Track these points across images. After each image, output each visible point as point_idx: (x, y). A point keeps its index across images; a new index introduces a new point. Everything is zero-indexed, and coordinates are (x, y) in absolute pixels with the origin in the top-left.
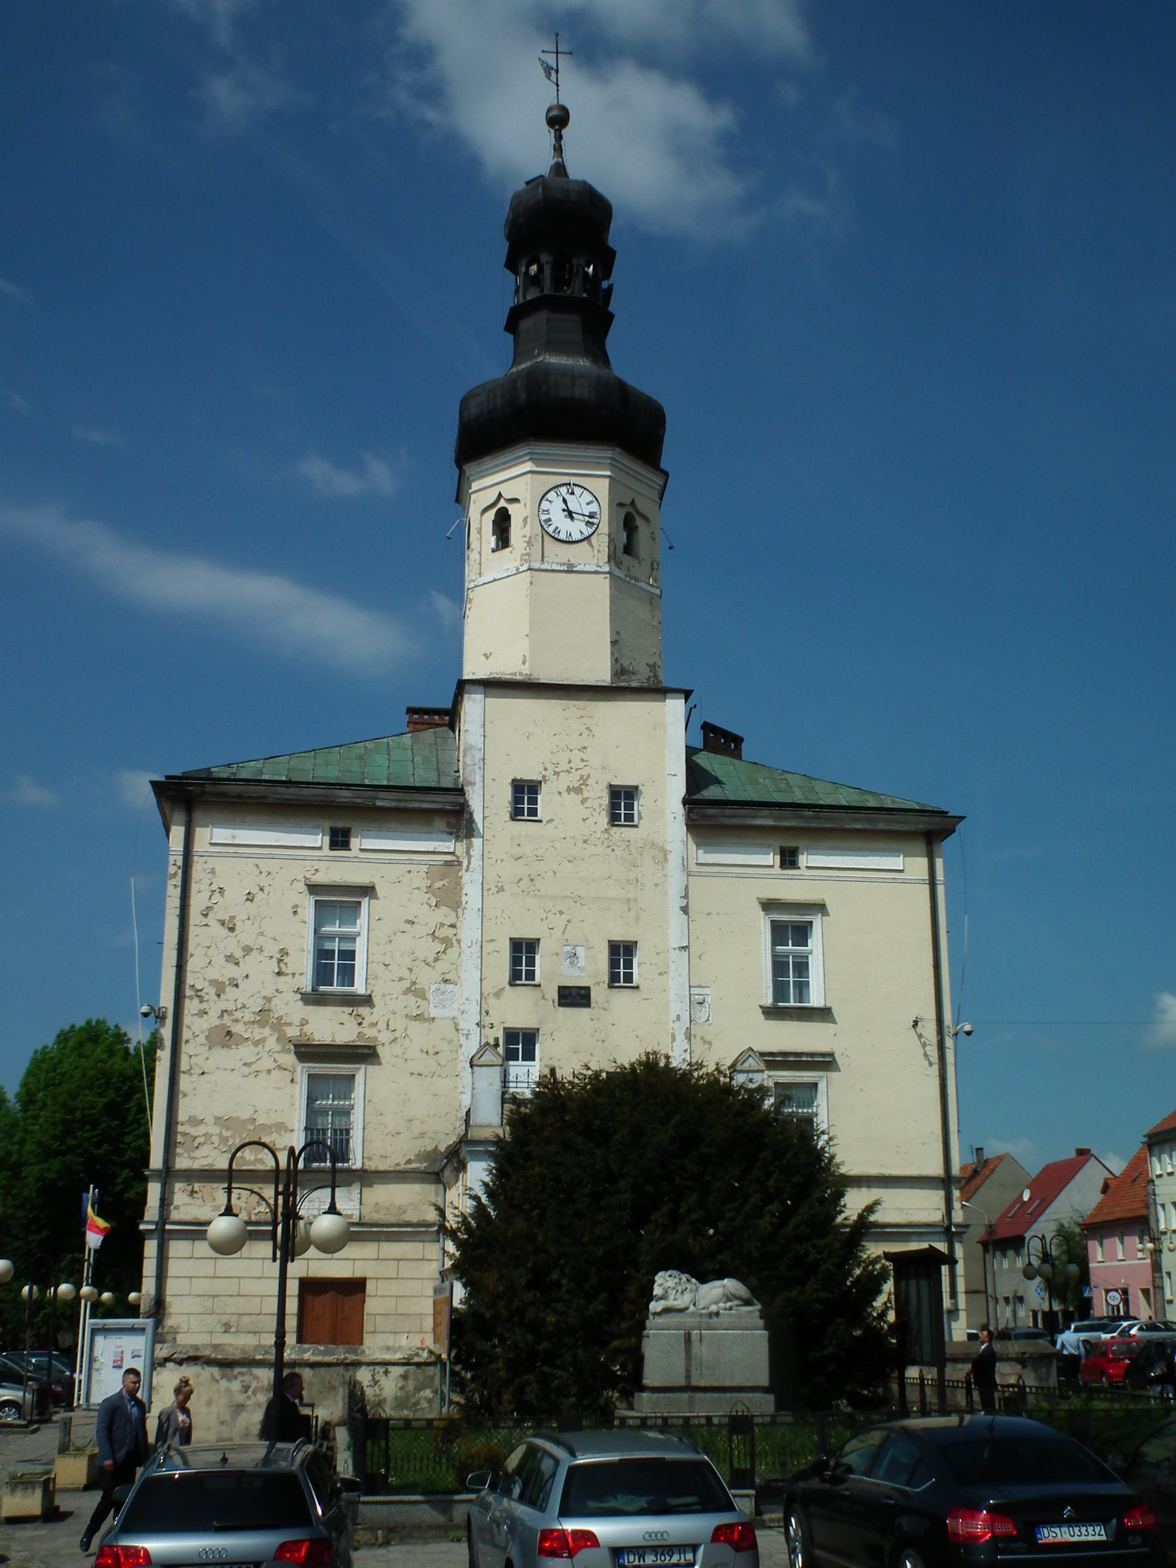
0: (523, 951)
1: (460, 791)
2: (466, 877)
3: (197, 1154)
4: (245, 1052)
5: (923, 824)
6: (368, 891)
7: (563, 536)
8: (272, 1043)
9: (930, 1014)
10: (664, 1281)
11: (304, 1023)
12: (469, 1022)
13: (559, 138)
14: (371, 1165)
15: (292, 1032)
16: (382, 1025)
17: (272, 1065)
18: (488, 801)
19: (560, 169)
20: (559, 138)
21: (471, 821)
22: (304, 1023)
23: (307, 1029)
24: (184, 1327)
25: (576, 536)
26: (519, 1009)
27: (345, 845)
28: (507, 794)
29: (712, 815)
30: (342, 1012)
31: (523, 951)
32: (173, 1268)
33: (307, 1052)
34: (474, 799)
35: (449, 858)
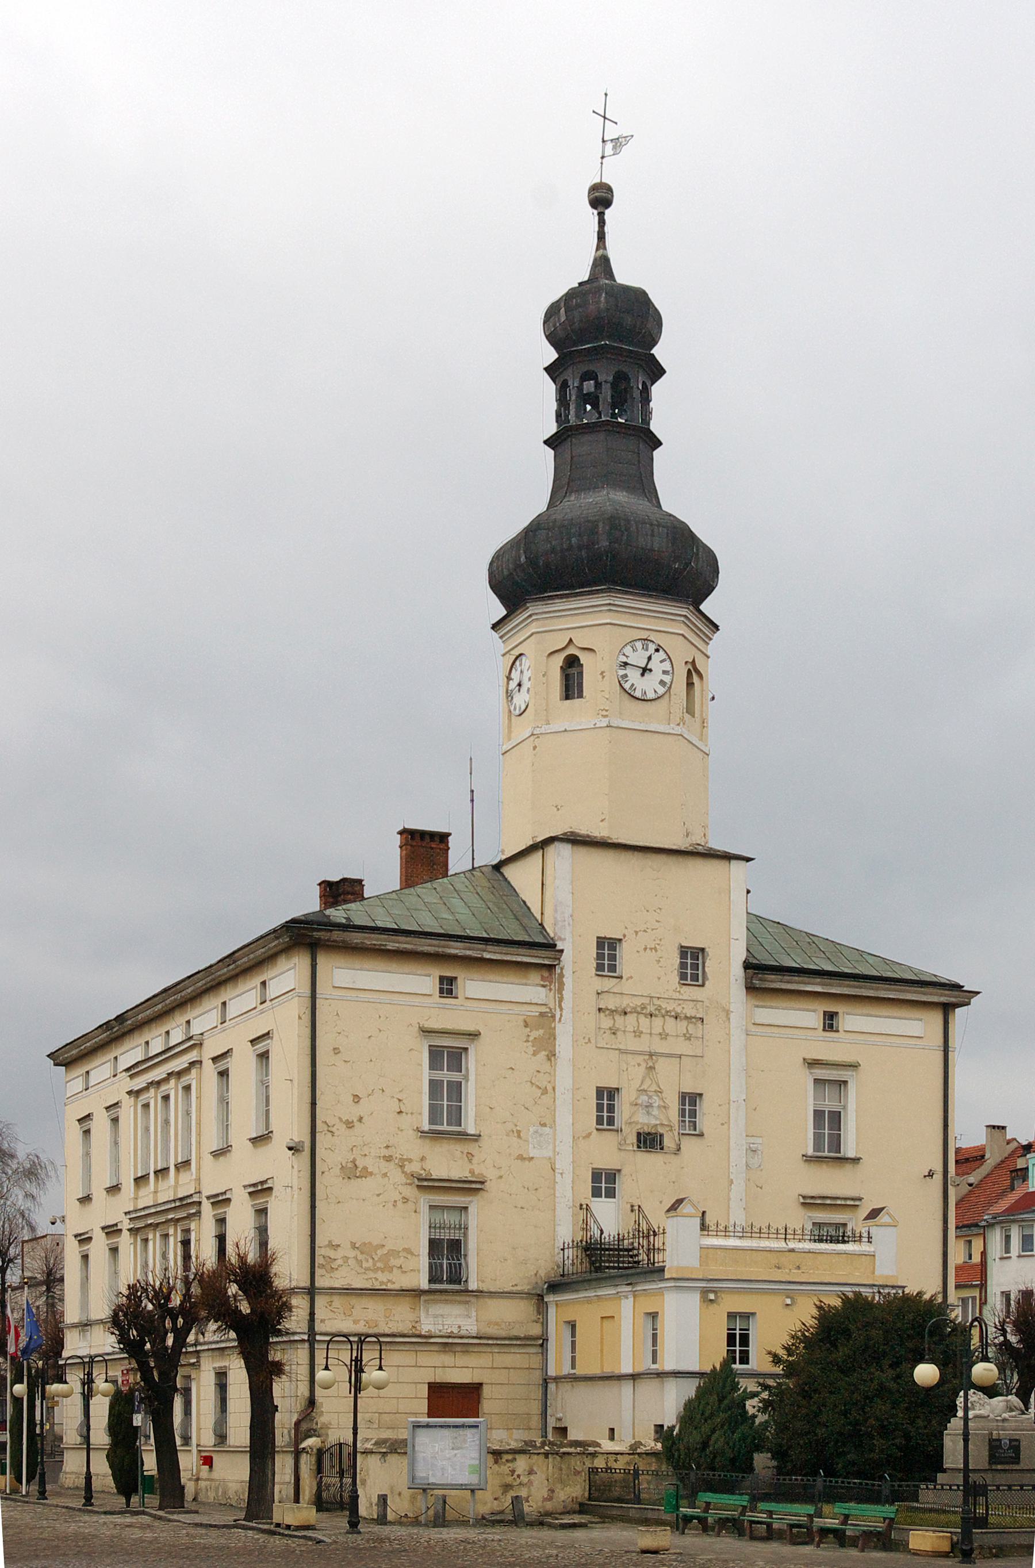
0: (607, 1096)
2: (559, 1029)
3: (337, 1274)
7: (638, 694)
8: (397, 1176)
11: (423, 1159)
12: (564, 1163)
13: (602, 223)
14: (484, 1287)
15: (414, 1167)
17: (398, 1197)
19: (602, 265)
20: (602, 223)
21: (562, 975)
22: (423, 1159)
23: (428, 1165)
24: (334, 1423)
25: (651, 695)
26: (606, 1151)
29: (764, 977)
31: (607, 1096)
33: (427, 1184)
35: (544, 1009)
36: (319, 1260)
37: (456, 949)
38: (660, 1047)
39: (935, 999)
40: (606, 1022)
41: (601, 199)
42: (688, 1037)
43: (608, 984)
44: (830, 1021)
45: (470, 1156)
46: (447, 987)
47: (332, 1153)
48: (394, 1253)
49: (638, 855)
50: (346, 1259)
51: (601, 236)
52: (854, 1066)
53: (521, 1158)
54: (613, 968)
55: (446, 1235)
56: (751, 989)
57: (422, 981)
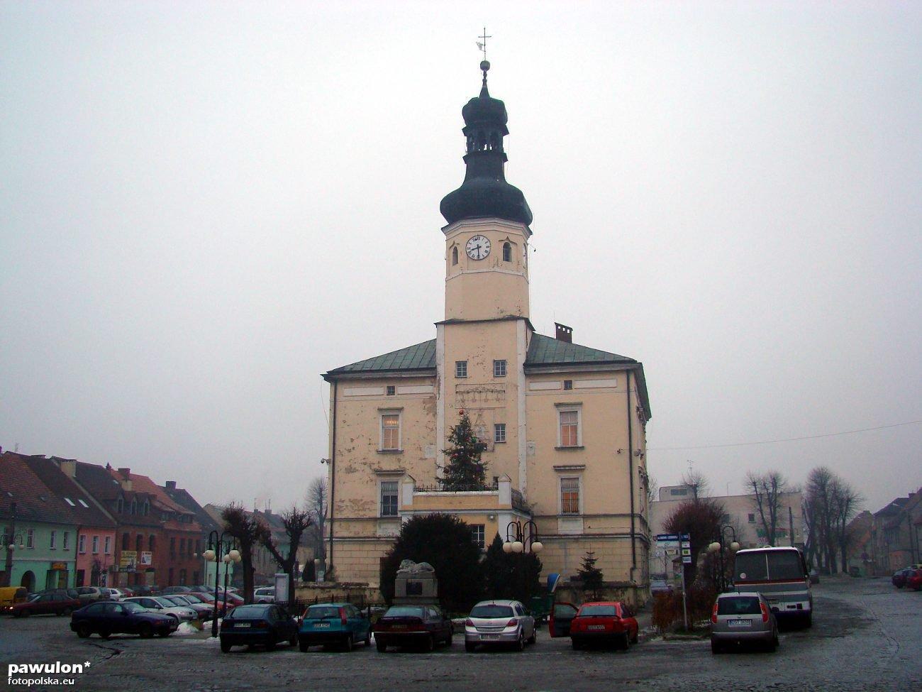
1: (435, 369)
3: (343, 513)
4: (357, 475)
5: (629, 367)
6: (401, 409)
8: (368, 470)
9: (625, 447)
10: (403, 563)
11: (379, 462)
13: (485, 75)
15: (376, 467)
16: (407, 462)
18: (445, 368)
19: (484, 91)
20: (485, 75)
21: (439, 380)
23: (381, 465)
27: (393, 393)
28: (454, 367)
30: (393, 458)
32: (336, 554)
33: (379, 473)
34: (441, 370)
35: (432, 395)
36: (335, 508)
37: (390, 375)
38: (484, 405)
39: (623, 368)
40: (459, 397)
41: (485, 66)
42: (498, 400)
43: (460, 381)
44: (568, 385)
45: (399, 460)
46: (391, 391)
47: (341, 464)
48: (366, 503)
49: (490, 325)
50: (347, 506)
51: (485, 81)
52: (580, 404)
53: (421, 459)
54: (465, 374)
55: (390, 494)
56: (528, 375)
57: (380, 390)
